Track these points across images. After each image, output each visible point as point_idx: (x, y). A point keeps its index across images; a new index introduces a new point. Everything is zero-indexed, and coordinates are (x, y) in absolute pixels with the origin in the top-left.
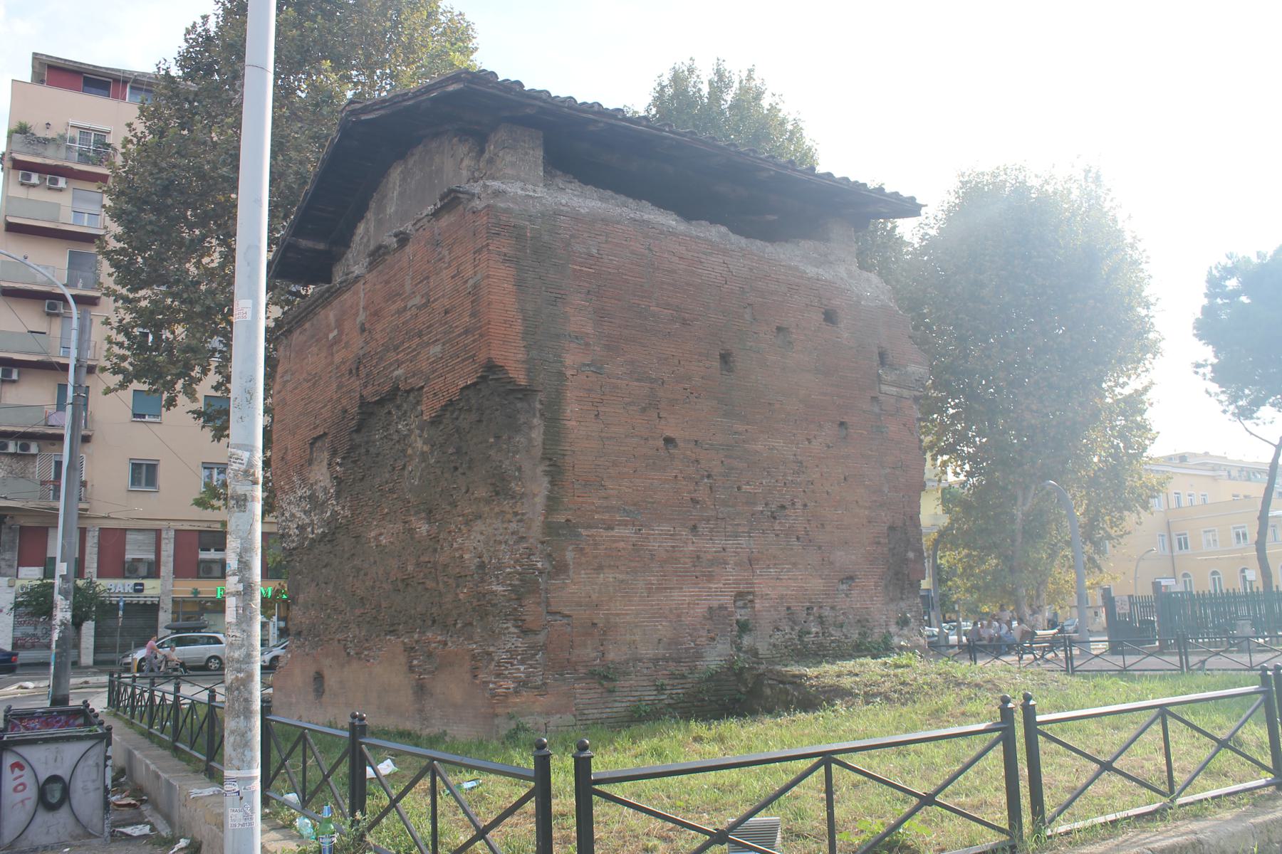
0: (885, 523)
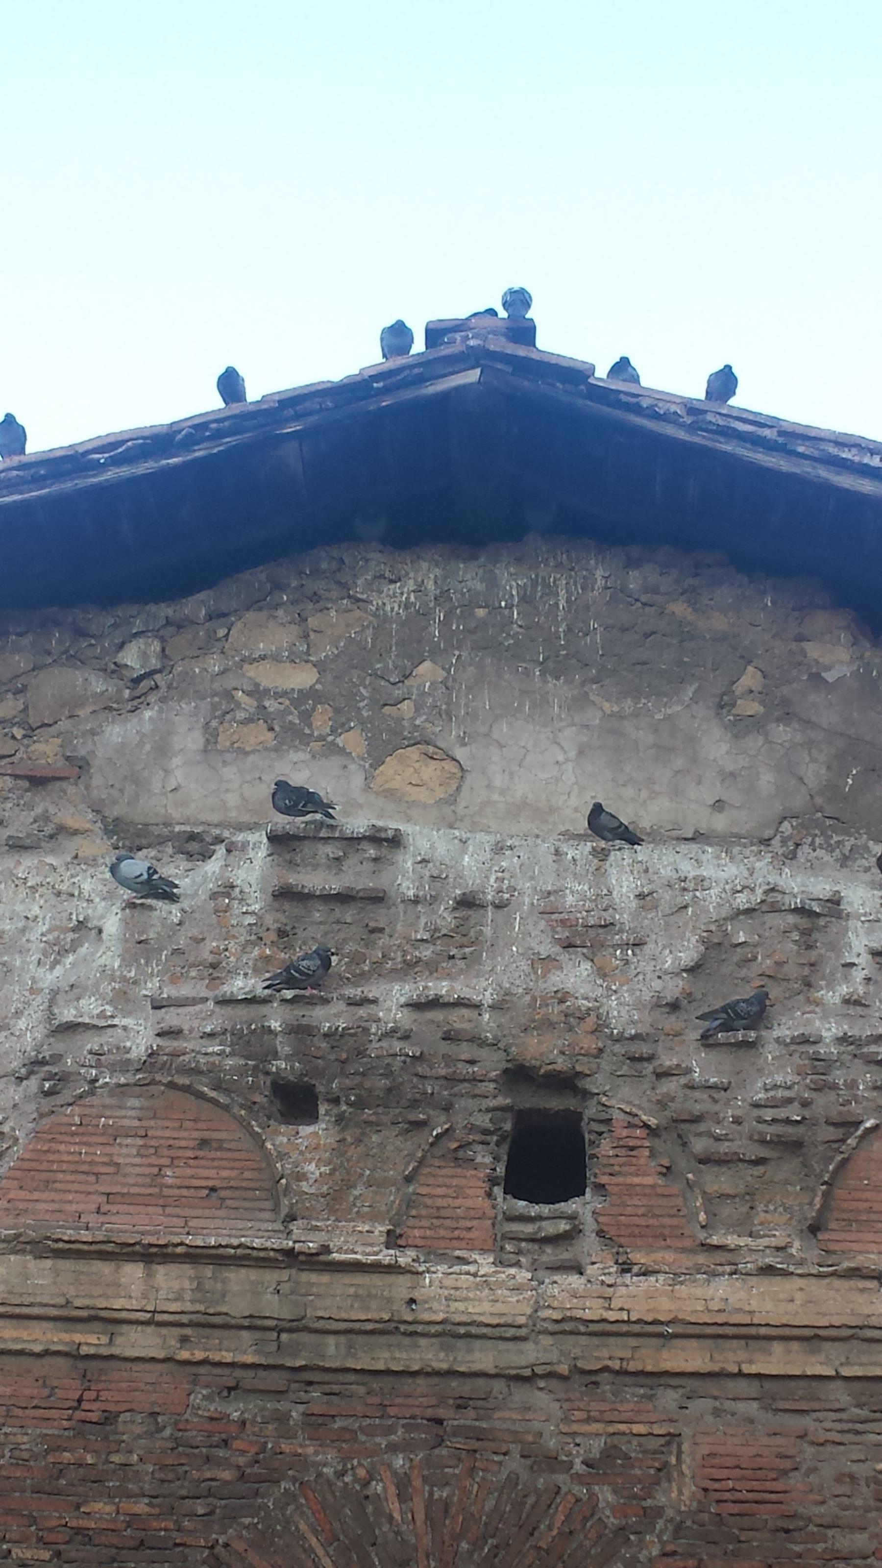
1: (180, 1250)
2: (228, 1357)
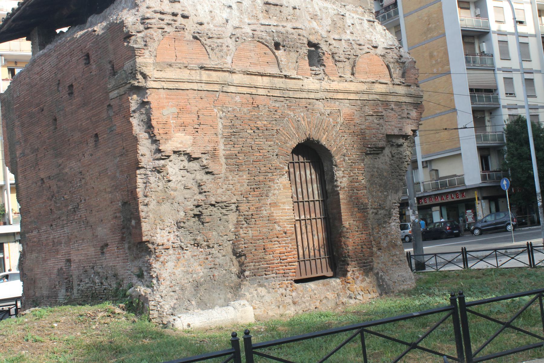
0: (118, 201)
1: (268, 74)
2: (276, 95)
